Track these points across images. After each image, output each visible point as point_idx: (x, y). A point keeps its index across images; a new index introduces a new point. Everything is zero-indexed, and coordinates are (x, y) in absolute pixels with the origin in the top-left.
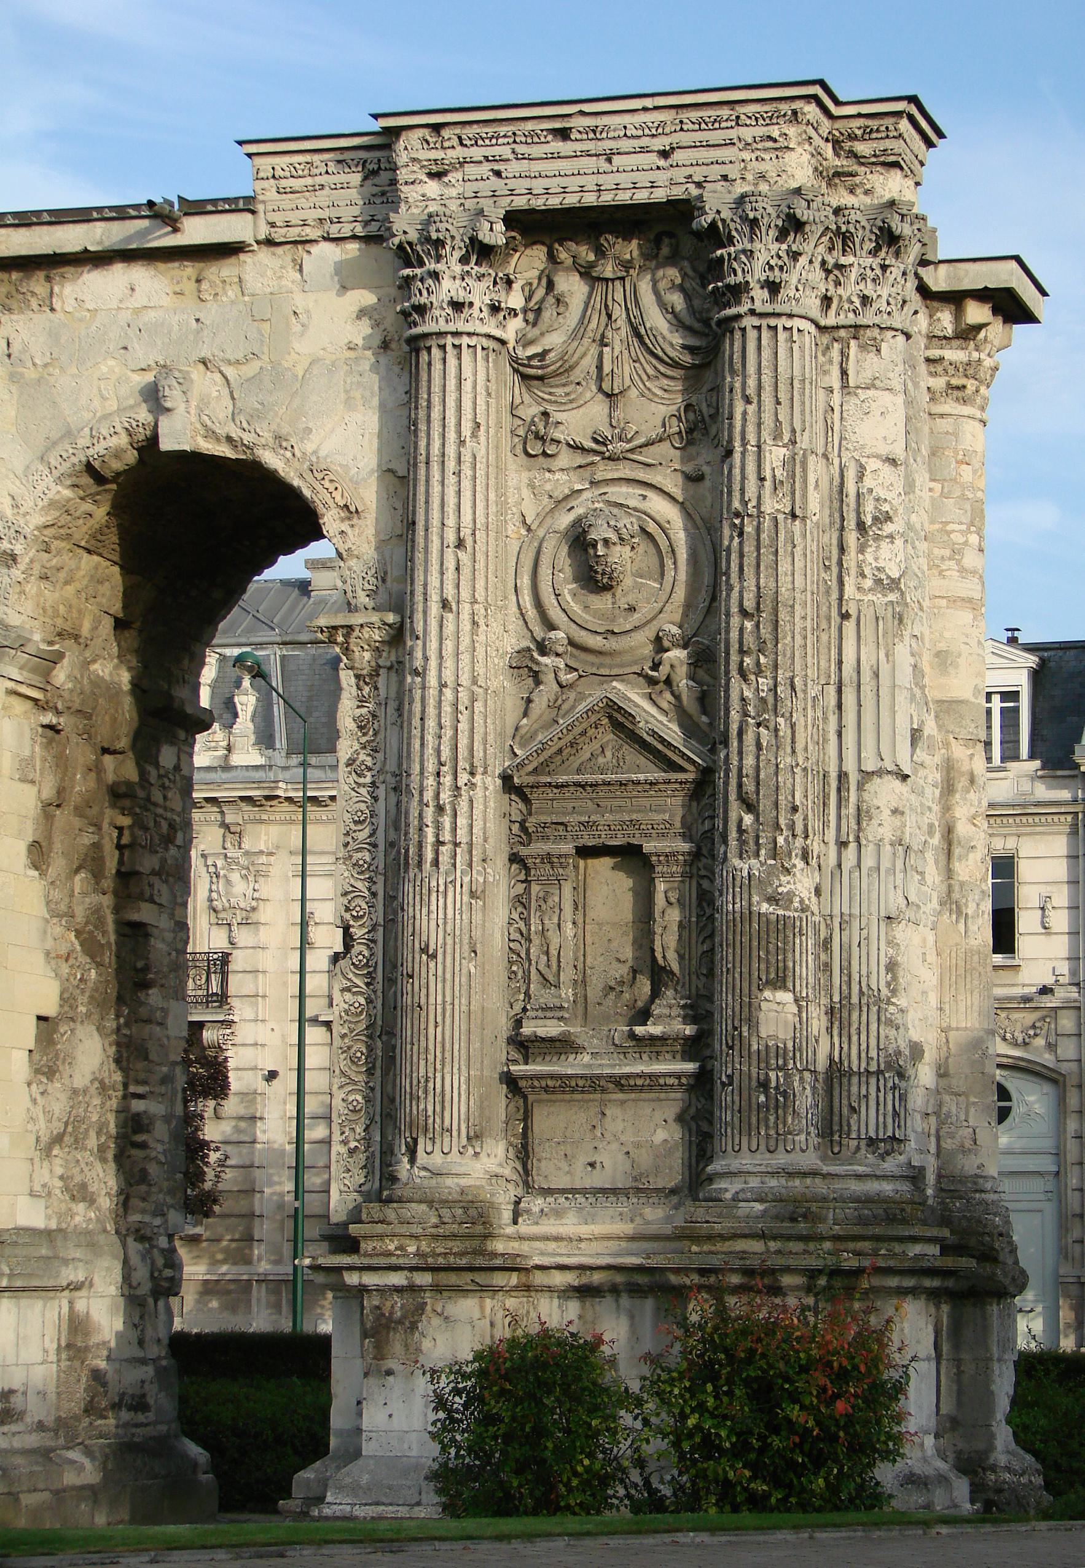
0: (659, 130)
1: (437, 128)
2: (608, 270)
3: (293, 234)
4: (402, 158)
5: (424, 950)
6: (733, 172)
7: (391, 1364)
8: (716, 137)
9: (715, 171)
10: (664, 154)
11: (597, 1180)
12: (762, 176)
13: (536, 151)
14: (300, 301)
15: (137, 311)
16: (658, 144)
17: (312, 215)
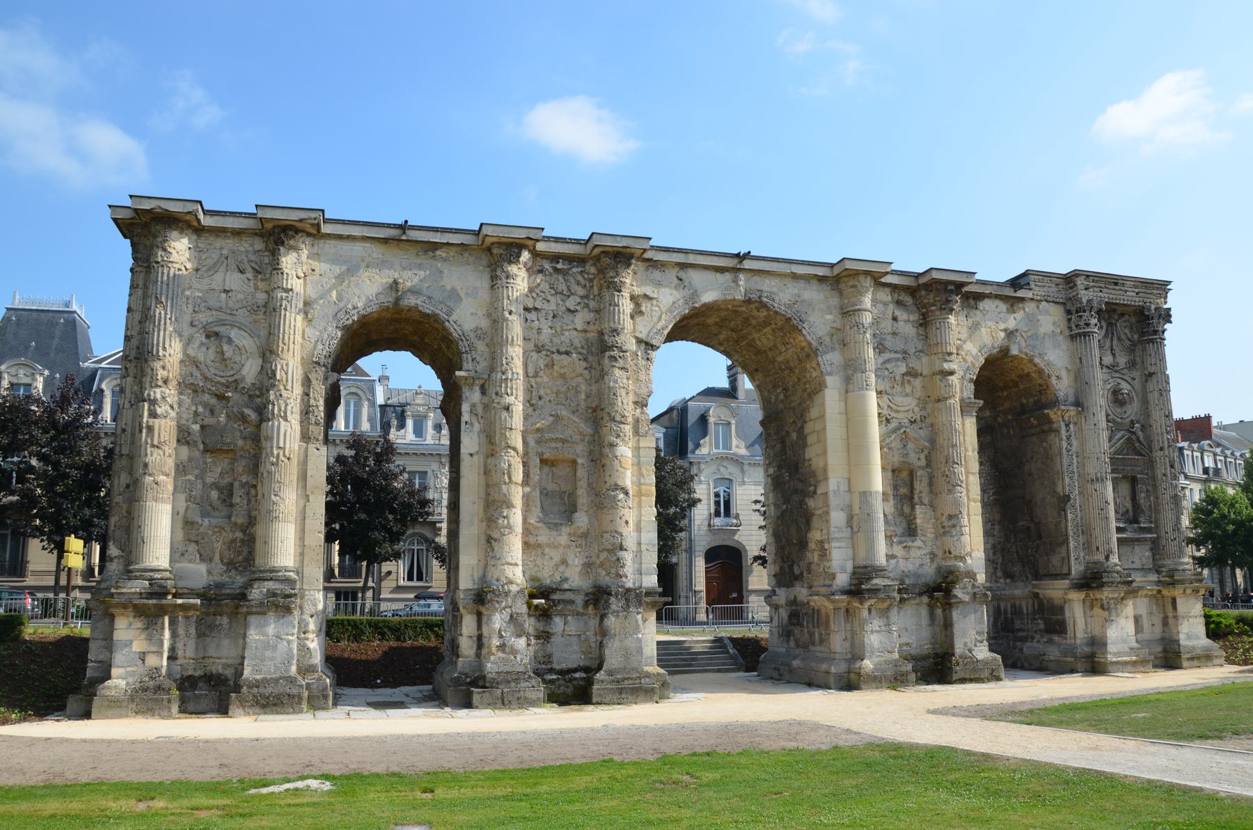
0: (1136, 287)
1: (1088, 276)
2: (1113, 321)
3: (1039, 298)
4: (1079, 283)
5: (1106, 502)
6: (1152, 301)
7: (1112, 618)
8: (1149, 291)
9: (1149, 300)
10: (1137, 294)
11: (1134, 566)
12: (1158, 303)
13: (1111, 287)
14: (1040, 317)
15: (999, 313)
16: (1136, 290)
17: (1043, 294)
